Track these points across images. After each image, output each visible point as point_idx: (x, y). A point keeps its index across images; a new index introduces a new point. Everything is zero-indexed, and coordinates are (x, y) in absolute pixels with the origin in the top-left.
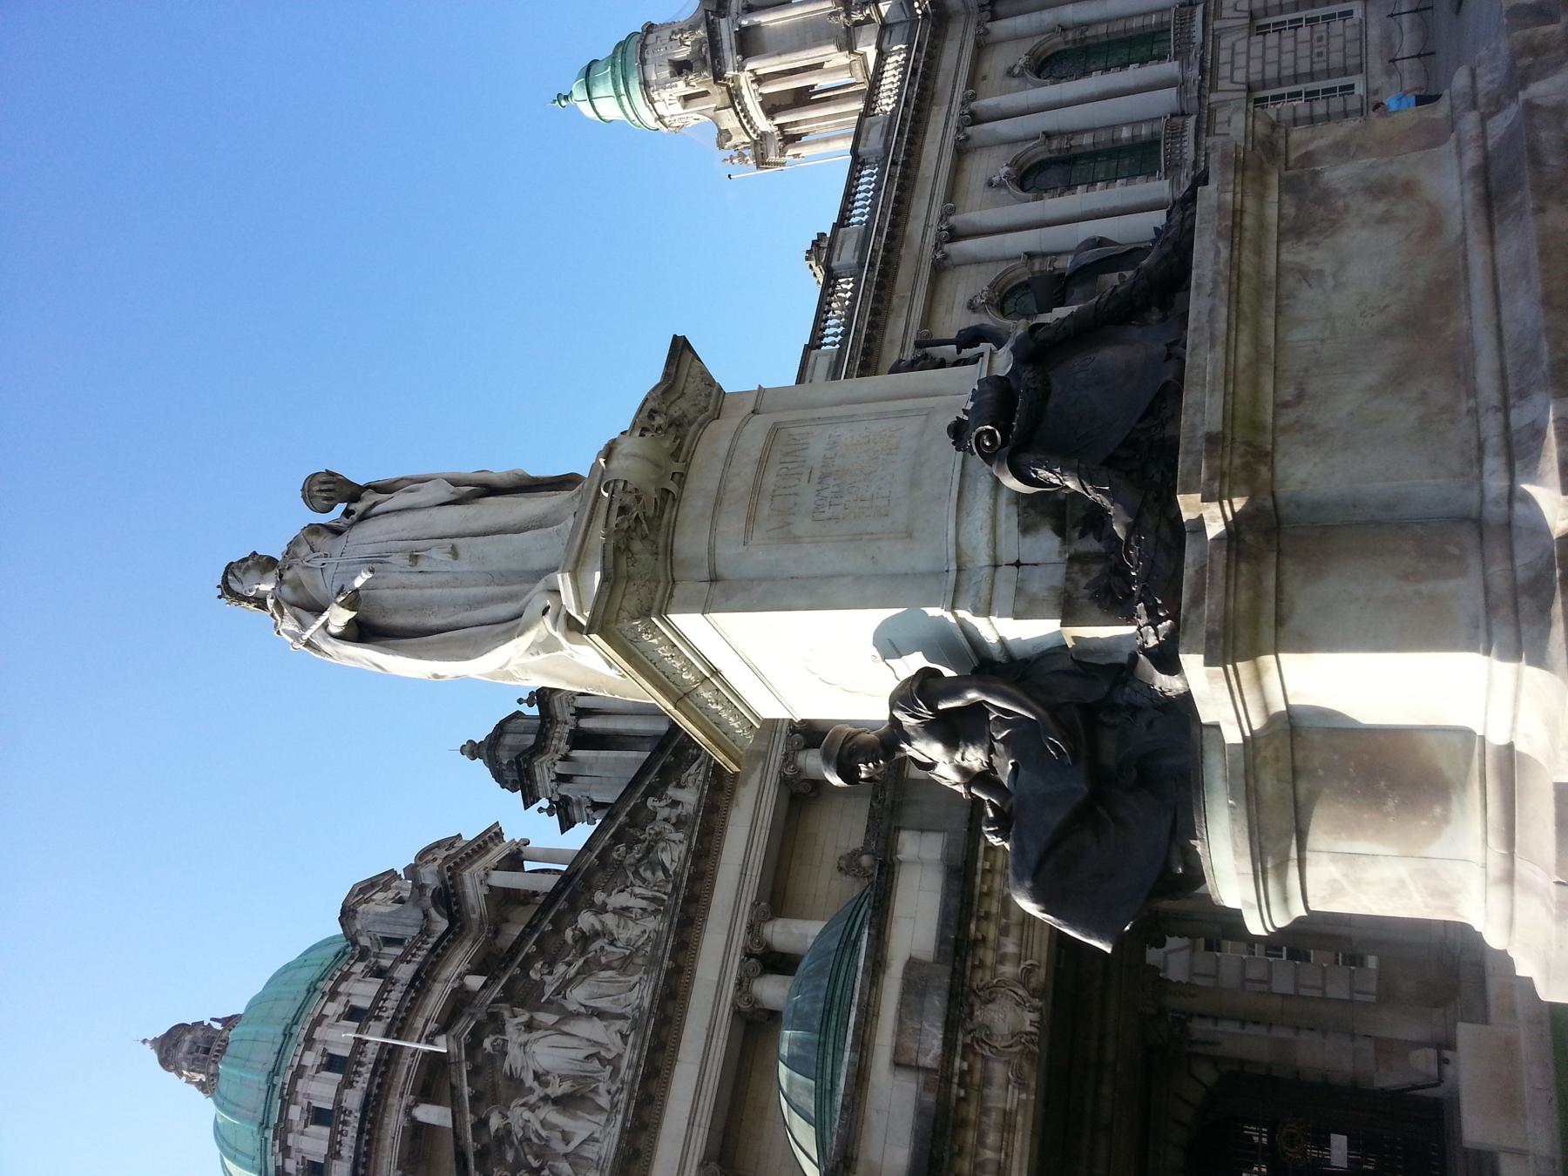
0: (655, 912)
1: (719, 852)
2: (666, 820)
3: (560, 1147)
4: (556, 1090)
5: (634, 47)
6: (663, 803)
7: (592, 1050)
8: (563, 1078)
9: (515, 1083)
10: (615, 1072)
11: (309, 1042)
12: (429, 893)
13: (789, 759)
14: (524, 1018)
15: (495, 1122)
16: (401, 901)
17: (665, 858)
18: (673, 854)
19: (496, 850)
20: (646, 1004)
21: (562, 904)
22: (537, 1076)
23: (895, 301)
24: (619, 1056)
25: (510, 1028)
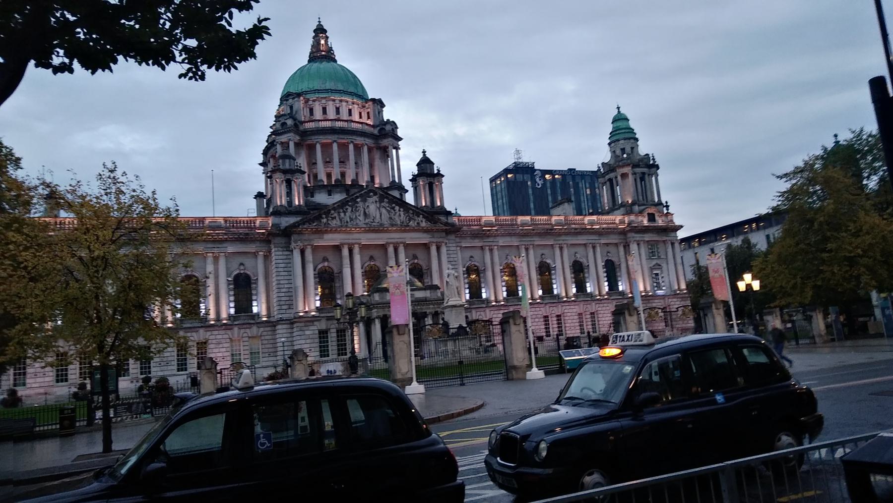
3: (357, 214)
4: (367, 211)
5: (631, 135)
9: (365, 201)
11: (341, 101)
12: (384, 127)
15: (358, 200)
16: (379, 113)
17: (411, 223)
19: (395, 142)
21: (399, 202)
25: (376, 198)
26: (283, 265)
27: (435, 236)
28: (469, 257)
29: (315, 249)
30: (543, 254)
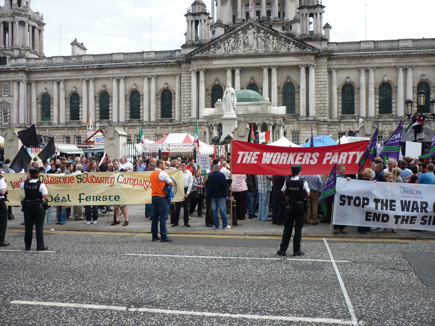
0: (274, 49)
1: (285, 57)
2: (289, 46)
6: (292, 45)
7: (252, 46)
8: (248, 41)
9: (246, 33)
10: (250, 50)
13: (302, 65)
14: (255, 32)
15: (240, 32)
18: (283, 50)
20: (260, 52)
21: (273, 32)
22: (247, 37)
23: (425, 58)
24: (252, 50)
25: (253, 30)
26: (186, 84)
27: (305, 60)
28: (345, 77)
29: (207, 71)
30: (423, 75)
